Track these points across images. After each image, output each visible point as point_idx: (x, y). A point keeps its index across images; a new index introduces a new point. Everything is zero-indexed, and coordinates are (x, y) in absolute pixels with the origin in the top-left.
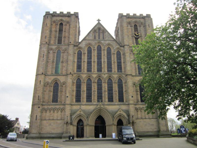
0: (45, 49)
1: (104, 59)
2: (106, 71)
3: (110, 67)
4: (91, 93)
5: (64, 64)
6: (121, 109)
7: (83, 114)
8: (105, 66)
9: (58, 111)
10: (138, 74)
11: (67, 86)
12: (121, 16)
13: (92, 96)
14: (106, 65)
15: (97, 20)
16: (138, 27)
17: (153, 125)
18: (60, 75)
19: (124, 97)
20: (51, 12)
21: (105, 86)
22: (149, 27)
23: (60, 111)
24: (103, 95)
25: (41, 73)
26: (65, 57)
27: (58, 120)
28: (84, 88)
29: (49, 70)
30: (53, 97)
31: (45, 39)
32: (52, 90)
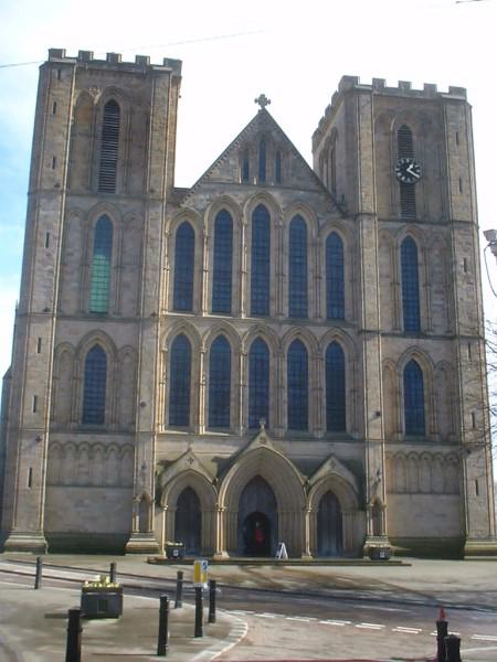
0: (53, 213)
1: (280, 263)
2: (286, 310)
3: (301, 296)
4: (229, 393)
5: (128, 277)
6: (336, 457)
7: (200, 471)
8: (280, 290)
9: (106, 456)
10: (403, 329)
11: (144, 363)
12: (349, 90)
13: (232, 404)
14: (286, 286)
15: (256, 101)
16: (414, 138)
17: (444, 515)
18: (113, 320)
19: (347, 412)
20: (72, 53)
21: (280, 368)
22: (458, 143)
23: (112, 455)
24: (272, 400)
25: (41, 310)
26: (129, 246)
27: (107, 486)
28: (202, 372)
29: (67, 298)
30: (85, 403)
31: (51, 169)
32: (83, 376)
